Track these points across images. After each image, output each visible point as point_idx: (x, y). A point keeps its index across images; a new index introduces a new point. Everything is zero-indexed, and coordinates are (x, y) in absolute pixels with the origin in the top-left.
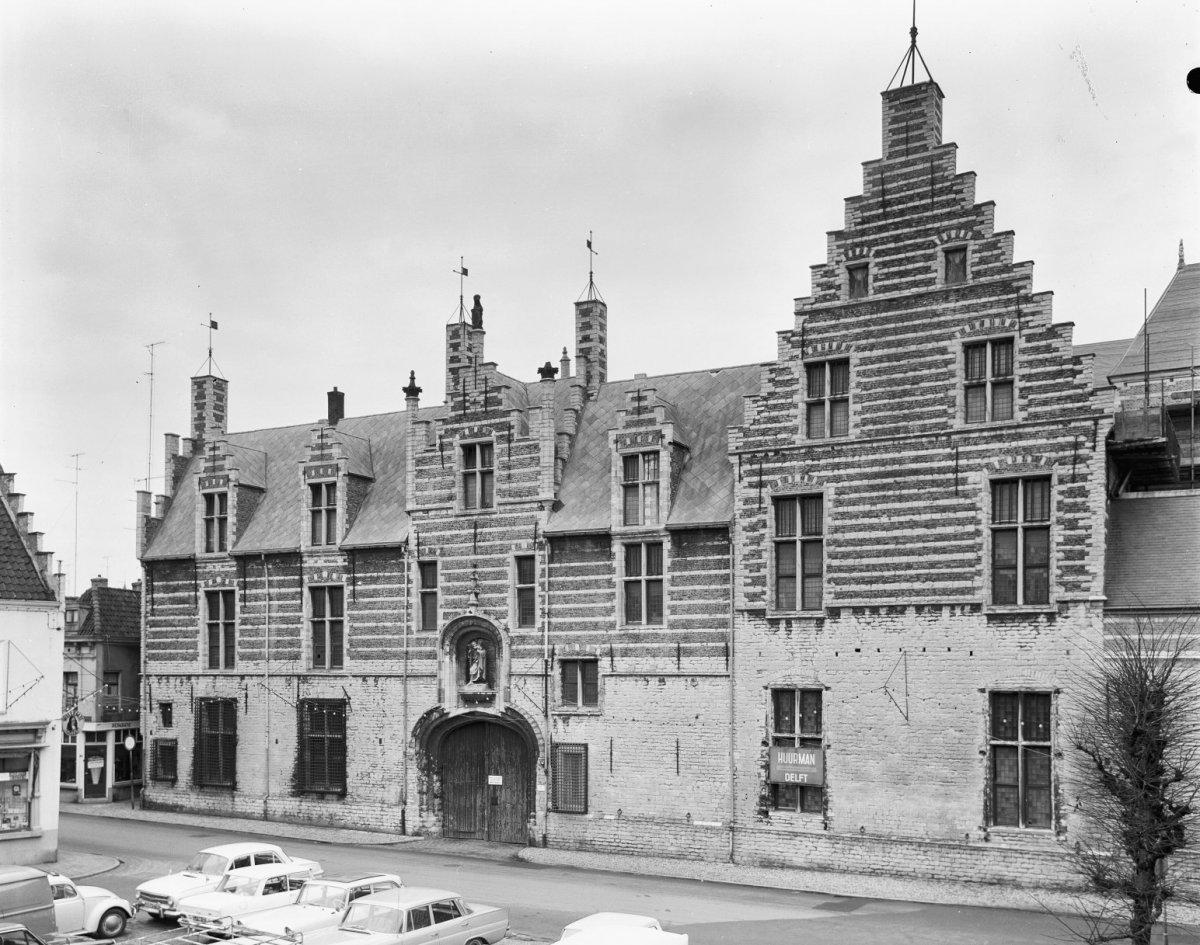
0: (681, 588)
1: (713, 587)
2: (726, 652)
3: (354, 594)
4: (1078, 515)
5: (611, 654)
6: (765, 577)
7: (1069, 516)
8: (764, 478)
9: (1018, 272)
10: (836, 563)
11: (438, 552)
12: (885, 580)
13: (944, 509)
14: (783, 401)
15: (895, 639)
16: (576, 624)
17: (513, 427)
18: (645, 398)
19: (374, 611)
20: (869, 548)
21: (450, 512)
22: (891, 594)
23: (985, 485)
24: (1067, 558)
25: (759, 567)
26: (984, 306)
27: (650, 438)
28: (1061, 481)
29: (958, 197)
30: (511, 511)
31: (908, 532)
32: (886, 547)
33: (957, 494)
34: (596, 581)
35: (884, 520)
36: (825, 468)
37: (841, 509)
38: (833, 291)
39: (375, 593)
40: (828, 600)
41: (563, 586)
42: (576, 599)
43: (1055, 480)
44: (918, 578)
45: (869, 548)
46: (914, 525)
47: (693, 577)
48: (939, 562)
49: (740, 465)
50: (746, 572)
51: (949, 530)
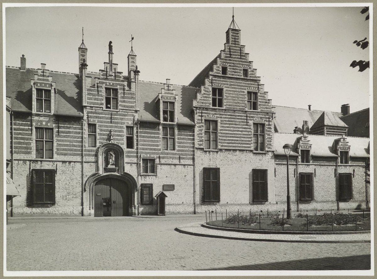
0: (180, 141)
1: (189, 141)
2: (193, 159)
3: (58, 132)
4: (270, 133)
5: (159, 158)
6: (203, 140)
7: (268, 133)
8: (203, 114)
9: (258, 79)
10: (221, 138)
11: (97, 121)
12: (232, 143)
13: (245, 128)
14: (207, 96)
15: (235, 158)
16: (148, 148)
17: (125, 86)
18: (170, 87)
19: (69, 139)
20: (228, 135)
21: (101, 109)
22: (234, 147)
23: (252, 124)
24: (268, 142)
25: (202, 137)
26: (252, 84)
27: (172, 98)
28: (267, 125)
29: (246, 58)
30: (125, 112)
31: (237, 133)
32: (233, 135)
33: (247, 125)
34: (155, 136)
35: (232, 129)
36: (218, 114)
37: (222, 125)
38: (219, 72)
39: (69, 132)
40: (219, 147)
41: (144, 137)
42: (148, 141)
43: (266, 125)
44: (239, 143)
45: (228, 135)
46: (238, 131)
47: (184, 138)
48: (244, 140)
49: (196, 110)
50: (198, 138)
51: (246, 133)
